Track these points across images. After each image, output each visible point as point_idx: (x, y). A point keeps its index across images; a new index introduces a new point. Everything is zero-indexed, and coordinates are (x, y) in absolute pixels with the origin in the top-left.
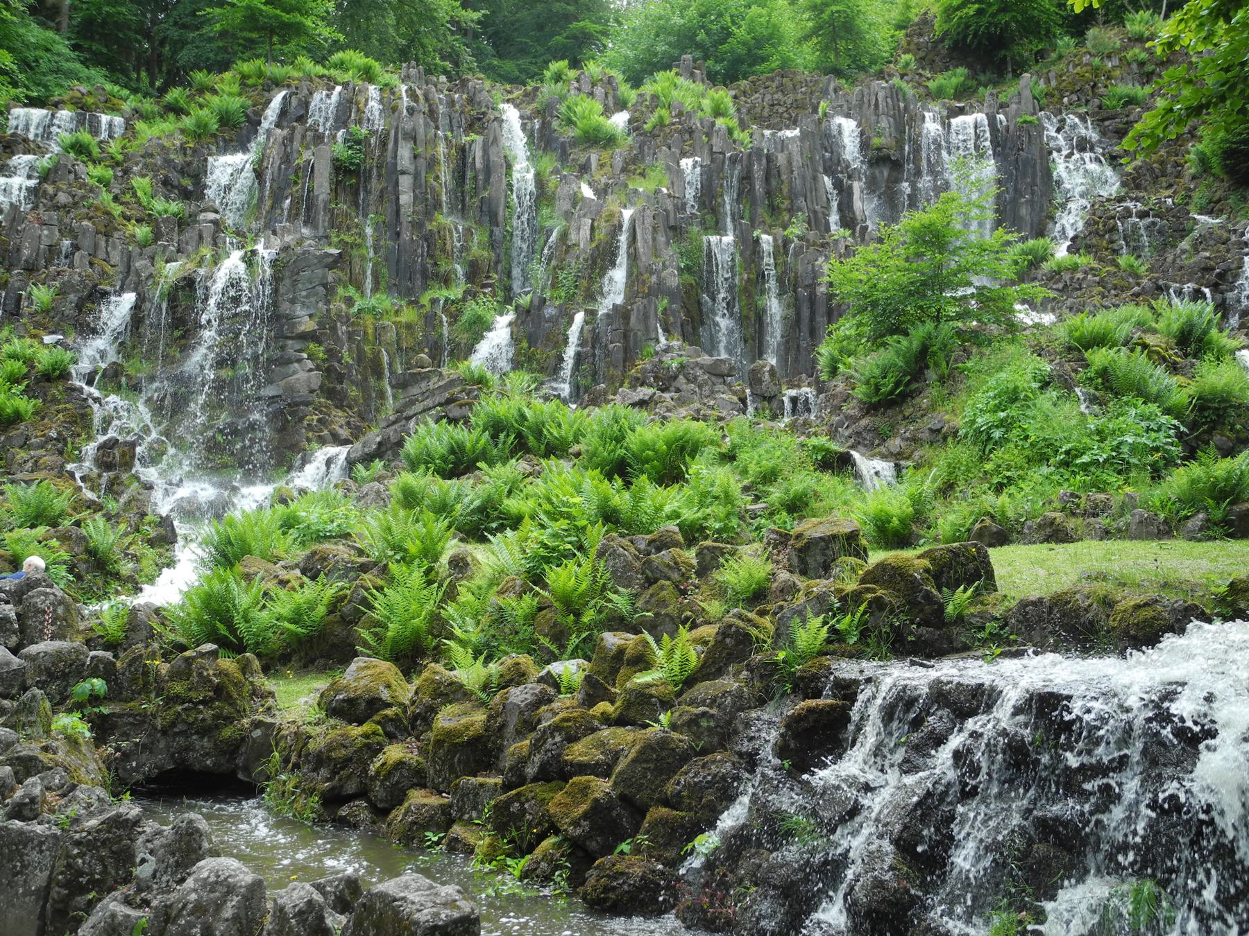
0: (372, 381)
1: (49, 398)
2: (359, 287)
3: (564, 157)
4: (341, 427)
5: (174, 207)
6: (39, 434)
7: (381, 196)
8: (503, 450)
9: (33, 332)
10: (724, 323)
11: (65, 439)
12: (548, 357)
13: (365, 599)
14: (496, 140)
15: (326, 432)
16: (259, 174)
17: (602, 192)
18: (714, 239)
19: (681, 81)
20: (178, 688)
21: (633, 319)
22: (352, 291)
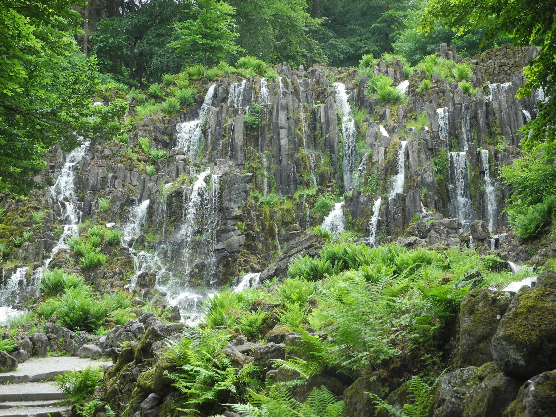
0: (270, 241)
1: (112, 254)
2: (261, 190)
3: (371, 112)
4: (255, 264)
5: (162, 153)
6: (110, 271)
7: (271, 141)
8: (337, 269)
9: (101, 222)
10: (461, 200)
11: (123, 273)
12: (363, 223)
13: (276, 317)
14: (331, 106)
15: (248, 266)
16: (204, 132)
17: (391, 131)
18: (454, 154)
19: (440, 60)
21: (407, 201)
22: (257, 193)
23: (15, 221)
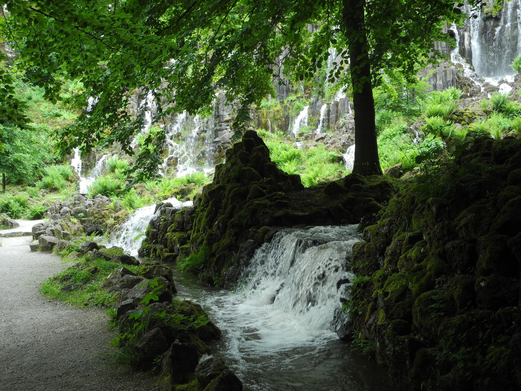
20: (96, 215)
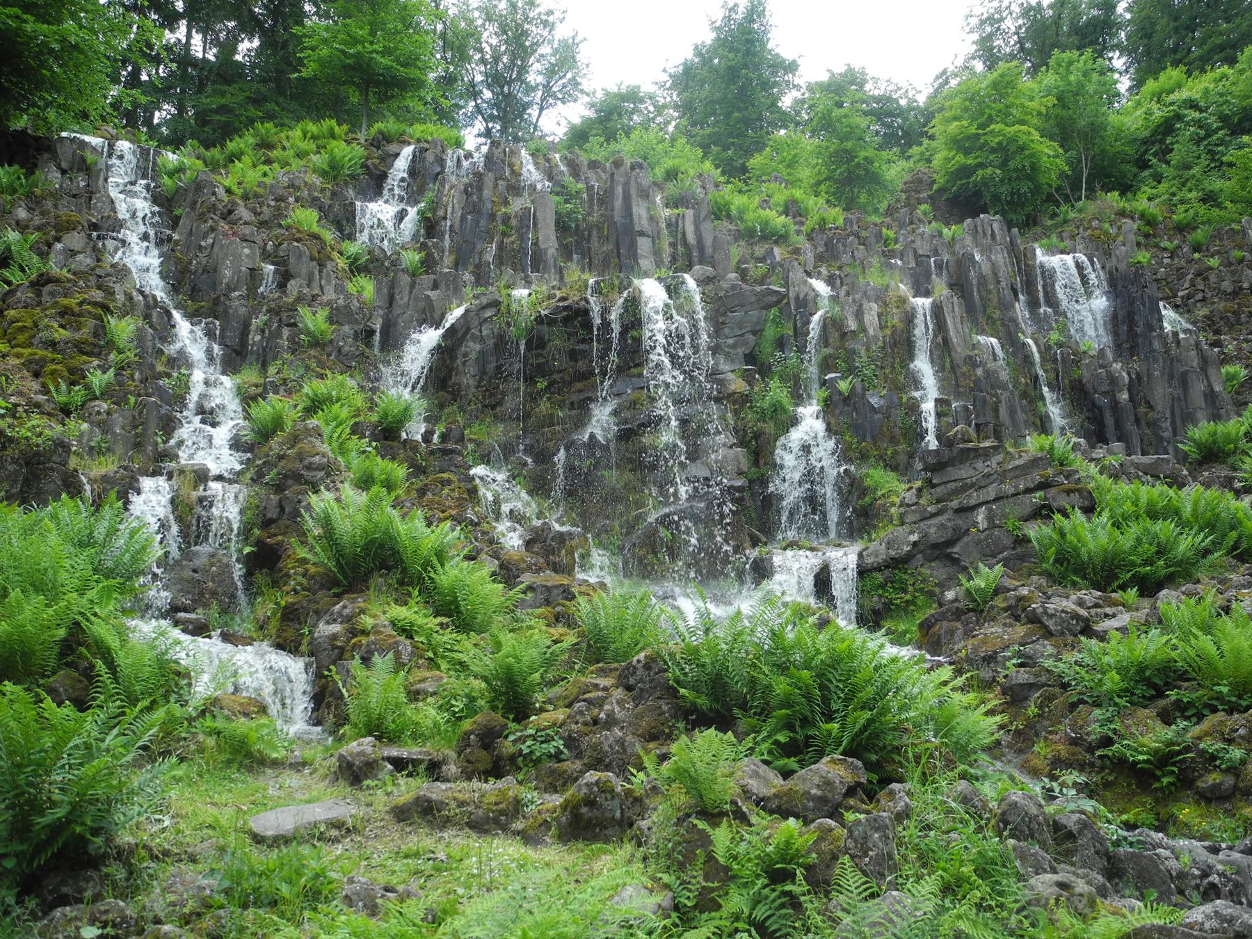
6: (442, 515)
21: (1003, 412)
23: (44, 335)
